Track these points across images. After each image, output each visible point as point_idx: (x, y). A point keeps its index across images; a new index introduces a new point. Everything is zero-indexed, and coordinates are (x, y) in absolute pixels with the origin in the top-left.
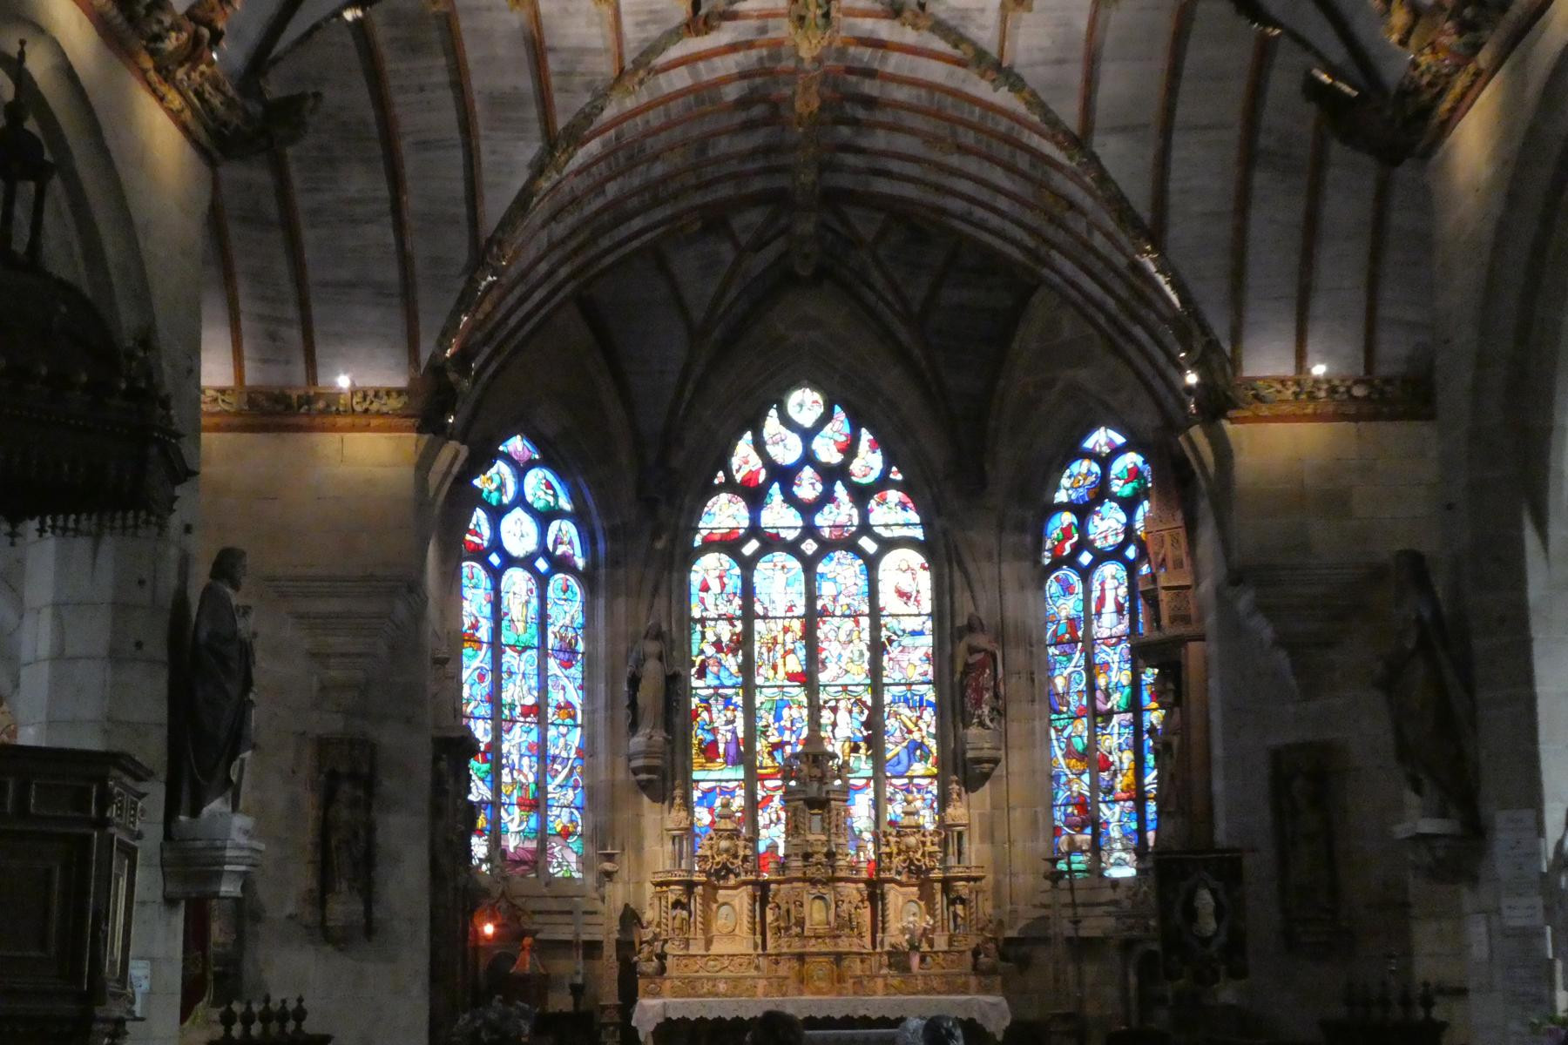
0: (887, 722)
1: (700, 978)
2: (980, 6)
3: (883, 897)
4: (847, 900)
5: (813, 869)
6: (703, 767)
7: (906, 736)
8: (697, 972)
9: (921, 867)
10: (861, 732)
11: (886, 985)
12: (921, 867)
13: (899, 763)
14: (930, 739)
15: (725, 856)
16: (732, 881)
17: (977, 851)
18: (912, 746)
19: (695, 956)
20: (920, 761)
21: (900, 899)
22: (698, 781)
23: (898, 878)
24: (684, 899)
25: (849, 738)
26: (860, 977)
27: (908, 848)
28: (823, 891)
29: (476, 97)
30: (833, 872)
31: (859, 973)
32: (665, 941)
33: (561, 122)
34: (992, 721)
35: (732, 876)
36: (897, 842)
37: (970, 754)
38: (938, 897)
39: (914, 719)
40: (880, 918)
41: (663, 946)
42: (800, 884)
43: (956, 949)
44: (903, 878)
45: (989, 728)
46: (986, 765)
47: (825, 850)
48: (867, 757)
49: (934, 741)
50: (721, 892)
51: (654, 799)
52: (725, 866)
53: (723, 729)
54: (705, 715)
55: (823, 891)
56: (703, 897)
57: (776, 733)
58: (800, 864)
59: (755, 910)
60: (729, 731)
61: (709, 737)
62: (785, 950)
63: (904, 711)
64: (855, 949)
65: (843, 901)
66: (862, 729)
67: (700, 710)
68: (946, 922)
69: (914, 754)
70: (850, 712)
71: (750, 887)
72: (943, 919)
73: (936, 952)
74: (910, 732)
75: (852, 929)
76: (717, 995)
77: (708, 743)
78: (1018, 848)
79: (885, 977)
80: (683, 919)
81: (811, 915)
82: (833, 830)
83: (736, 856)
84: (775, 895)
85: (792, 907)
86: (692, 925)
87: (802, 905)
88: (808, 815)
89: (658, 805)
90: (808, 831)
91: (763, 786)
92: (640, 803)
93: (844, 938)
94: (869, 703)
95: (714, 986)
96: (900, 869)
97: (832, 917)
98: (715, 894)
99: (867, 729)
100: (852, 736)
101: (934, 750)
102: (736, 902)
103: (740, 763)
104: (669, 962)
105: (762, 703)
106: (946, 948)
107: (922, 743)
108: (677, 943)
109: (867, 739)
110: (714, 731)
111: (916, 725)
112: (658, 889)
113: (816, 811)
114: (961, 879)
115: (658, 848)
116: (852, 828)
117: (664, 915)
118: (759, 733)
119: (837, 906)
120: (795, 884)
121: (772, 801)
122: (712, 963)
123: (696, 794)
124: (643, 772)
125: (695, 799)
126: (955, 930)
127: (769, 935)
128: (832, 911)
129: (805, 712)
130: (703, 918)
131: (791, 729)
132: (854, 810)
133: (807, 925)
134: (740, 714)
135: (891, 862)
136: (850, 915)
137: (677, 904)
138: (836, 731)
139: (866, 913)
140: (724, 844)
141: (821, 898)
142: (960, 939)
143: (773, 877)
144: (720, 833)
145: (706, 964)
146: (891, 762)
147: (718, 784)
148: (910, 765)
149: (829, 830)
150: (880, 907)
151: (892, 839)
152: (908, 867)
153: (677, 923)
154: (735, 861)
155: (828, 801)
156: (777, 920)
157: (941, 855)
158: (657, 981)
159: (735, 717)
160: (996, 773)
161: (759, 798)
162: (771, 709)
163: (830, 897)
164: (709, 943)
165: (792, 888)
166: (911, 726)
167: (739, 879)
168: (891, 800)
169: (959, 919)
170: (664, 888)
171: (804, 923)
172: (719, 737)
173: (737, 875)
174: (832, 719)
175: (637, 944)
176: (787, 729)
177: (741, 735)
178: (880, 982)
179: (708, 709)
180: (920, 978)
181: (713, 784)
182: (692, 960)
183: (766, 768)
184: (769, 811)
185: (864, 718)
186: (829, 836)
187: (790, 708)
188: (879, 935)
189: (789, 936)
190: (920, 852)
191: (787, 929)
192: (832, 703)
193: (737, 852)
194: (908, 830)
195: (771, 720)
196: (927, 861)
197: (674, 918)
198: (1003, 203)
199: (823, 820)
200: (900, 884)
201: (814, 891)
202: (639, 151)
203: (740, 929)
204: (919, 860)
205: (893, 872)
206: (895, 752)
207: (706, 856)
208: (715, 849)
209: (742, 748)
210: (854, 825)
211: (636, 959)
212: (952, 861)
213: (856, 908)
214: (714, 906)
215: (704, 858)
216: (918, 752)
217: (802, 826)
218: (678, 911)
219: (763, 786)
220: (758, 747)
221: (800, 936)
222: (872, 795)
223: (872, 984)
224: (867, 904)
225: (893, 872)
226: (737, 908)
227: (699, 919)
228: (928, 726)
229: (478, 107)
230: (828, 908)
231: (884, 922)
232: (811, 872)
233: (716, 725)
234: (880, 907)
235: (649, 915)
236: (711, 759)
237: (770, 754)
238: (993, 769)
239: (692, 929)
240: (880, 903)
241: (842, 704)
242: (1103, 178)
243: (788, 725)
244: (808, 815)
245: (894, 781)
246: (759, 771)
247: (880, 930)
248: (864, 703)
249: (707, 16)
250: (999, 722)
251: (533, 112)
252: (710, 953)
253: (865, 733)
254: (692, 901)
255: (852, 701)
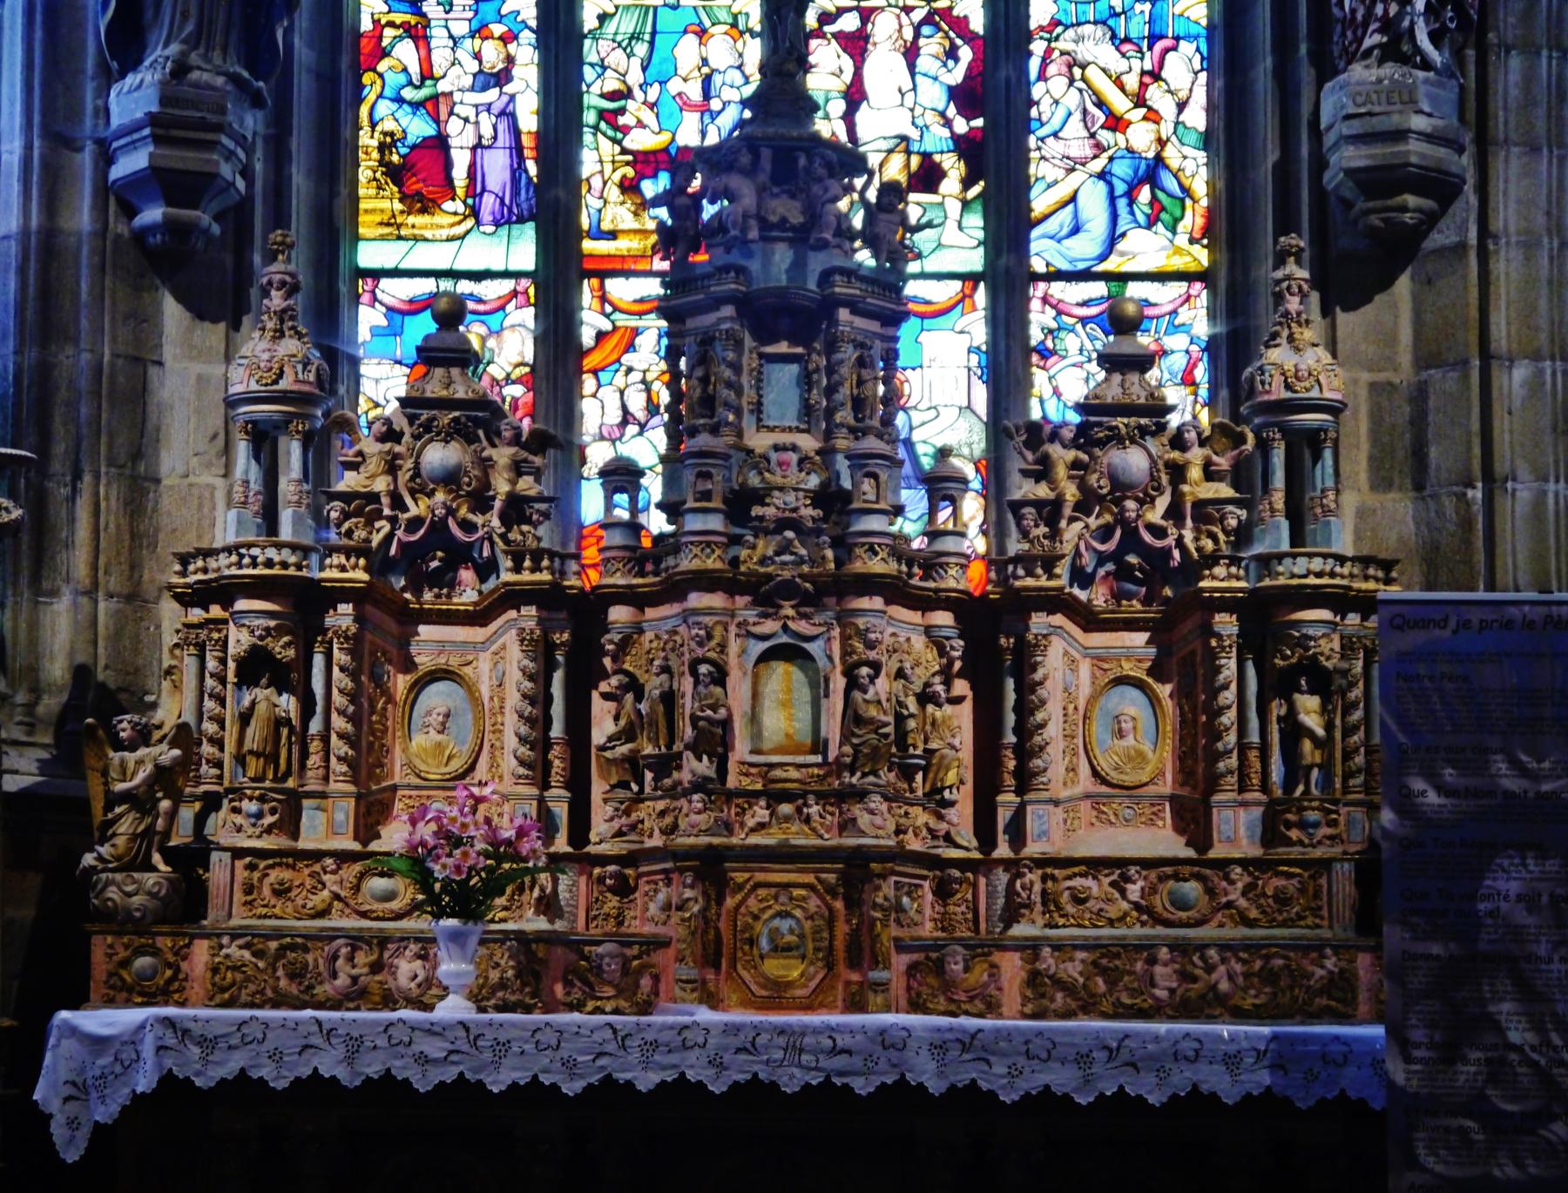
0: (1037, 91)
1: (330, 936)
3: (1024, 661)
4: (891, 665)
5: (766, 546)
6: (393, 229)
7: (1105, 136)
8: (323, 913)
9: (1167, 552)
10: (948, 123)
11: (1034, 979)
12: (1167, 552)
13: (1076, 230)
14: (1187, 151)
15: (440, 496)
16: (468, 593)
17: (1362, 514)
18: (1122, 169)
19: (317, 856)
20: (1151, 222)
21: (1085, 668)
22: (377, 274)
23: (1082, 595)
24: (283, 650)
25: (904, 139)
26: (937, 946)
27: (1121, 486)
28: (802, 627)
30: (839, 563)
31: (928, 930)
32: (211, 803)
34: (1435, 38)
35: (467, 575)
36: (1075, 465)
37: (1353, 157)
38: (1229, 667)
39: (1132, 82)
40: (1011, 738)
41: (200, 820)
42: (716, 600)
43: (1295, 852)
44: (1098, 596)
45: (1426, 65)
46: (1411, 200)
47: (813, 481)
48: (966, 204)
49: (1202, 156)
50: (425, 631)
51: (200, 310)
52: (438, 527)
53: (467, 103)
54: (406, 52)
55: (802, 627)
56: (355, 645)
57: (648, 117)
58: (715, 523)
59: (549, 699)
60: (488, 107)
61: (419, 128)
62: (657, 841)
63: (1097, 50)
64: (915, 845)
65: (876, 667)
66: (952, 111)
67: (389, 33)
68: (1253, 755)
69: (1131, 196)
70: (911, 54)
71: (531, 611)
72: (1243, 747)
73: (1223, 864)
74: (1116, 123)
75: (907, 773)
76: (389, 1000)
77: (413, 147)
78: (1524, 494)
79: (1031, 948)
80: (279, 722)
81: (754, 719)
82: (845, 415)
83: (481, 501)
84: (625, 645)
85: (687, 684)
86: (315, 746)
87: (720, 676)
88: (749, 361)
89: (215, 333)
90: (748, 422)
91: (603, 299)
92: (144, 324)
93: (876, 802)
94: (977, 24)
95: (376, 967)
96: (1088, 561)
97: (832, 728)
98: (404, 641)
99: (967, 112)
100: (914, 134)
101: (1200, 187)
102: (482, 671)
103: (521, 220)
104: (219, 870)
105: (603, 18)
106: (1256, 852)
107: (1159, 160)
108: (251, 807)
109: (964, 146)
110: (432, 106)
111: (1139, 101)
112: (196, 614)
113: (783, 347)
114: (1314, 598)
115: (210, 478)
116: (909, 444)
117: (209, 704)
118: (590, 117)
119: (853, 684)
120: (696, 600)
121: (630, 347)
122: (378, 884)
123: (369, 318)
124: (150, 200)
125: (363, 333)
126: (1289, 784)
127: (598, 788)
128: (836, 702)
129: (754, 51)
130: (351, 719)
131: (704, 108)
132: (914, 385)
133: (741, 749)
134: (526, 54)
135: (1055, 534)
136: (900, 719)
137: (255, 667)
138: (863, 116)
139: (962, 718)
140: (438, 456)
141: (792, 653)
142: (1313, 816)
143: (619, 580)
144: (425, 415)
145: (357, 888)
146: (1050, 226)
147: (446, 285)
148: (1113, 239)
149: (830, 413)
150: (1011, 697)
151: (1062, 456)
152: (1117, 556)
153: (255, 735)
154: (478, 519)
155: (829, 305)
156: (628, 734)
157: (1243, 514)
158: (165, 943)
159: (510, 60)
160: (1439, 238)
161: (587, 337)
162: (635, 37)
163: (826, 649)
164: (373, 811)
165: (686, 615)
166: (1120, 104)
167: (491, 583)
168: (1045, 354)
169: (1307, 745)
170: (216, 611)
171: (726, 743)
172: (453, 126)
173: (486, 570)
174: (848, 77)
175: (98, 806)
176: (685, 104)
177: (528, 122)
178: (1012, 966)
179: (418, 34)
180: (1164, 953)
181: (426, 286)
182: (304, 875)
183: (613, 235)
184: (620, 380)
185: (957, 75)
186: (828, 435)
187: (702, 33)
188: (1008, 798)
189: (673, 792)
190: (1163, 502)
191: (666, 764)
192: (850, 23)
193: (486, 484)
194: (1120, 422)
195: (635, 77)
196: (1188, 536)
197: (245, 718)
199: (806, 381)
200: (1089, 620)
201: (770, 626)
203: (494, 765)
204: (1158, 532)
205: (1062, 569)
206: (1062, 192)
207: (374, 497)
208: (404, 477)
209: (532, 168)
210: (916, 437)
211: (88, 859)
212: (1277, 536)
213: (925, 698)
214: (401, 683)
215: (363, 505)
216: (1145, 194)
217: (726, 394)
218: (262, 694)
219: (603, 299)
220: (589, 163)
221: (713, 789)
222: (979, 333)
223: (980, 974)
224: (961, 687)
225: (1062, 569)
226: (485, 690)
227: (338, 722)
228: (1181, 106)
230: (819, 687)
231: (1025, 752)
232: (756, 553)
233: (443, 87)
234: (1011, 697)
235: (172, 709)
236: (423, 203)
237: (629, 187)
238: (1430, 221)
239: (314, 760)
240: (1010, 684)
241: (884, 27)
243: (694, 92)
244: (749, 361)
245: (1058, 289)
246: (588, 246)
247: (1009, 781)
248: (960, 25)
250: (1458, 55)
252: (374, 846)
253: (961, 126)
254: (318, 660)
255: (918, 15)
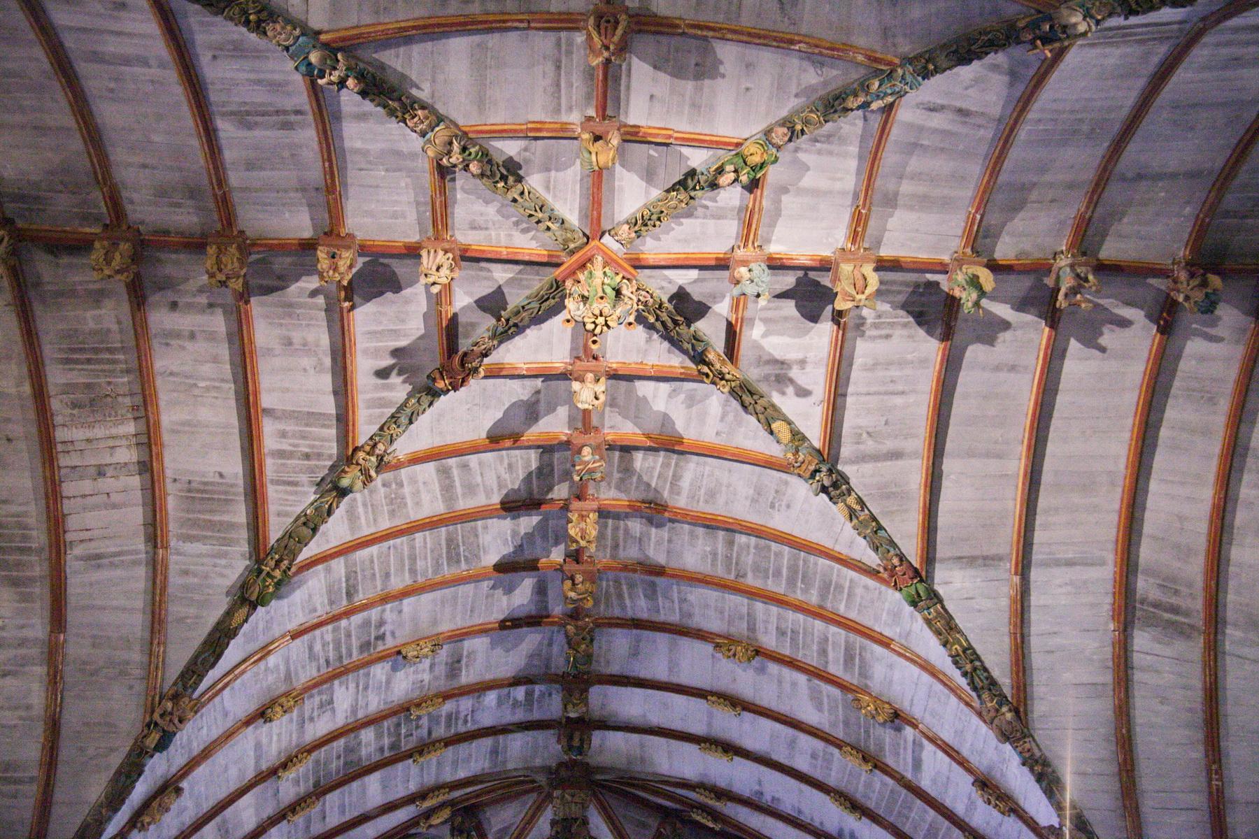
2: (800, 356)
29: (170, 487)
33: (275, 530)
198: (804, 753)
202: (377, 638)
229: (171, 503)
242: (946, 628)
249: (465, 354)
251: (240, 515)
